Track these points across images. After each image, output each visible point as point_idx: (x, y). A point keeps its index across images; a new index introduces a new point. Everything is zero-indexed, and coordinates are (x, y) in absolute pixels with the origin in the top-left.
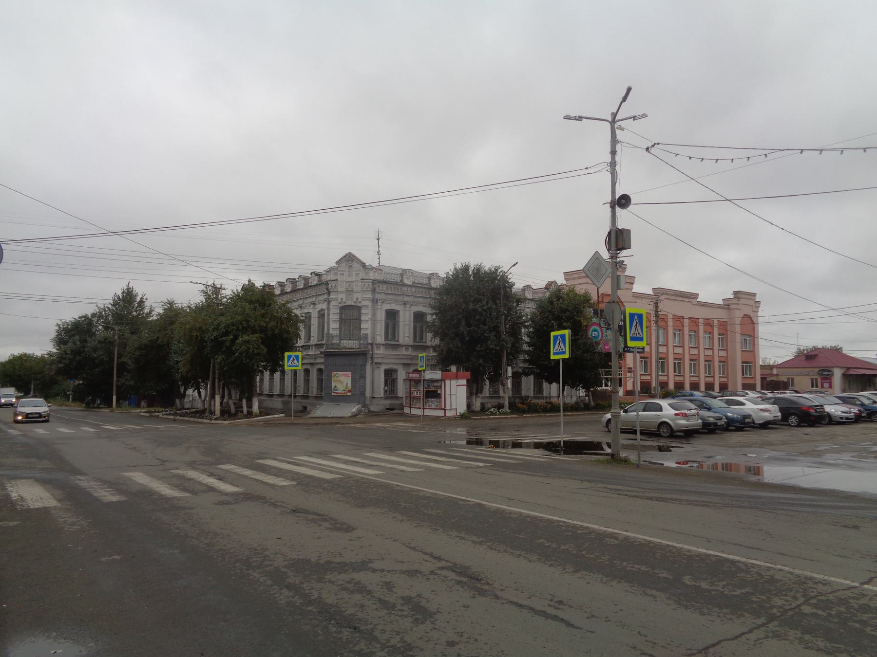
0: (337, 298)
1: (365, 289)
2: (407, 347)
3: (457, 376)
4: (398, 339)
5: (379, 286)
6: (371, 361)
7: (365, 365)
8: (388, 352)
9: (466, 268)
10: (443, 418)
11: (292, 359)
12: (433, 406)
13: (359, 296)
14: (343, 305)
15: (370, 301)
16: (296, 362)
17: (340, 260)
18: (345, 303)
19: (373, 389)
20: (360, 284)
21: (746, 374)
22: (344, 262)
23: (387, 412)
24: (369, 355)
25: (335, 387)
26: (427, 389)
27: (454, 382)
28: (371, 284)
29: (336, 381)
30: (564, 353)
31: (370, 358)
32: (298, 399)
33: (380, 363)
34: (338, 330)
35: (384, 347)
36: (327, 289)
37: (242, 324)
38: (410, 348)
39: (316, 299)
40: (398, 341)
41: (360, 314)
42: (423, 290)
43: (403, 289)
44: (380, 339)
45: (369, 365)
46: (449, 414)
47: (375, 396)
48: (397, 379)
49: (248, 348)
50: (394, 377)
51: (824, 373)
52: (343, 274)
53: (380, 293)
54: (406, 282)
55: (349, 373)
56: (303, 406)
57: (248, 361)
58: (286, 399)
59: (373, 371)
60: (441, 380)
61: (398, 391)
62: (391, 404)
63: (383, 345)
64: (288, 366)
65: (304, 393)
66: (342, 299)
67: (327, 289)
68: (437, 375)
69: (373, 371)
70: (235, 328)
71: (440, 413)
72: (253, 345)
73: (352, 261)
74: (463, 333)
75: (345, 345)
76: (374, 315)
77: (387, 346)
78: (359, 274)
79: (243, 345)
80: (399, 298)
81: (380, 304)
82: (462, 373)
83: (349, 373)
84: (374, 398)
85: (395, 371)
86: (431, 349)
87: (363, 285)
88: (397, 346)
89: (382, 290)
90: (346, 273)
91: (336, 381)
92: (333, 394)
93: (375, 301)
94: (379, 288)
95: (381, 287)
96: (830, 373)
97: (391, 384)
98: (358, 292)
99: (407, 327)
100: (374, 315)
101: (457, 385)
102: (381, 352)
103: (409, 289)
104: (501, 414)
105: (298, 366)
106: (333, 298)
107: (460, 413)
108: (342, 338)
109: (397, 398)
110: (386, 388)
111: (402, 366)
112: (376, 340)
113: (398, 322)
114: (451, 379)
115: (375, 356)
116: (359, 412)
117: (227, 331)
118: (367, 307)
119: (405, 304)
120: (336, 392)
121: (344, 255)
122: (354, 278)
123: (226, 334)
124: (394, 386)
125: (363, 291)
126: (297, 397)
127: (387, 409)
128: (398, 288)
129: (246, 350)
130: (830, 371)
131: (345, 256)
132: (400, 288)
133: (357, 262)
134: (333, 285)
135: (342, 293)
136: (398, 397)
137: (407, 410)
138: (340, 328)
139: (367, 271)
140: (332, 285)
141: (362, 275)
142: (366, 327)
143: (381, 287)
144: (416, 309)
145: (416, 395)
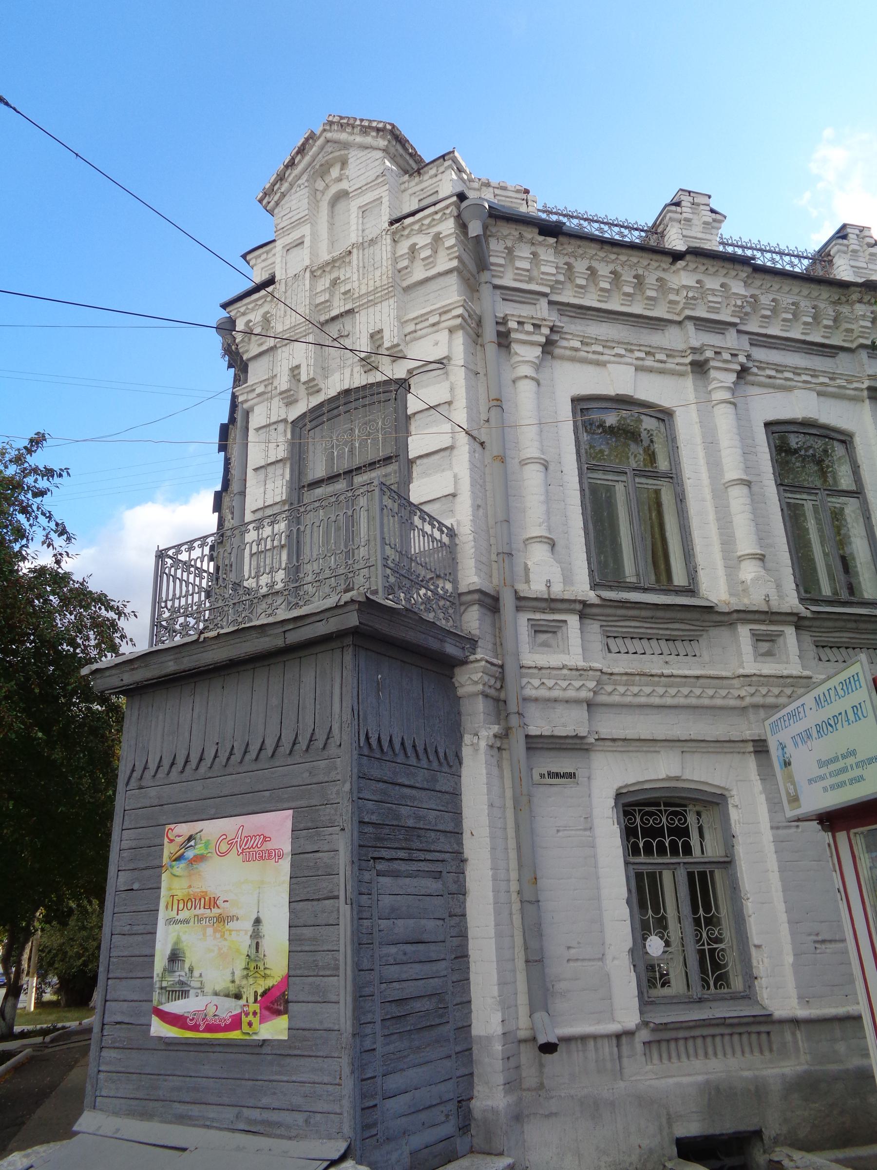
1: (419, 273)
4: (692, 572)
5: (510, 251)
6: (496, 729)
8: (621, 664)
17: (281, 178)
18: (312, 387)
25: (175, 957)
28: (448, 226)
45: (482, 757)
48: (728, 863)
53: (508, 293)
61: (761, 963)
63: (584, 610)
73: (344, 163)
92: (159, 1028)
97: (686, 908)
99: (738, 499)
102: (575, 658)
103: (713, 283)
110: (655, 945)
112: (527, 569)
113: (673, 477)
124: (712, 922)
125: (407, 289)
131: (302, 150)
136: (768, 1019)
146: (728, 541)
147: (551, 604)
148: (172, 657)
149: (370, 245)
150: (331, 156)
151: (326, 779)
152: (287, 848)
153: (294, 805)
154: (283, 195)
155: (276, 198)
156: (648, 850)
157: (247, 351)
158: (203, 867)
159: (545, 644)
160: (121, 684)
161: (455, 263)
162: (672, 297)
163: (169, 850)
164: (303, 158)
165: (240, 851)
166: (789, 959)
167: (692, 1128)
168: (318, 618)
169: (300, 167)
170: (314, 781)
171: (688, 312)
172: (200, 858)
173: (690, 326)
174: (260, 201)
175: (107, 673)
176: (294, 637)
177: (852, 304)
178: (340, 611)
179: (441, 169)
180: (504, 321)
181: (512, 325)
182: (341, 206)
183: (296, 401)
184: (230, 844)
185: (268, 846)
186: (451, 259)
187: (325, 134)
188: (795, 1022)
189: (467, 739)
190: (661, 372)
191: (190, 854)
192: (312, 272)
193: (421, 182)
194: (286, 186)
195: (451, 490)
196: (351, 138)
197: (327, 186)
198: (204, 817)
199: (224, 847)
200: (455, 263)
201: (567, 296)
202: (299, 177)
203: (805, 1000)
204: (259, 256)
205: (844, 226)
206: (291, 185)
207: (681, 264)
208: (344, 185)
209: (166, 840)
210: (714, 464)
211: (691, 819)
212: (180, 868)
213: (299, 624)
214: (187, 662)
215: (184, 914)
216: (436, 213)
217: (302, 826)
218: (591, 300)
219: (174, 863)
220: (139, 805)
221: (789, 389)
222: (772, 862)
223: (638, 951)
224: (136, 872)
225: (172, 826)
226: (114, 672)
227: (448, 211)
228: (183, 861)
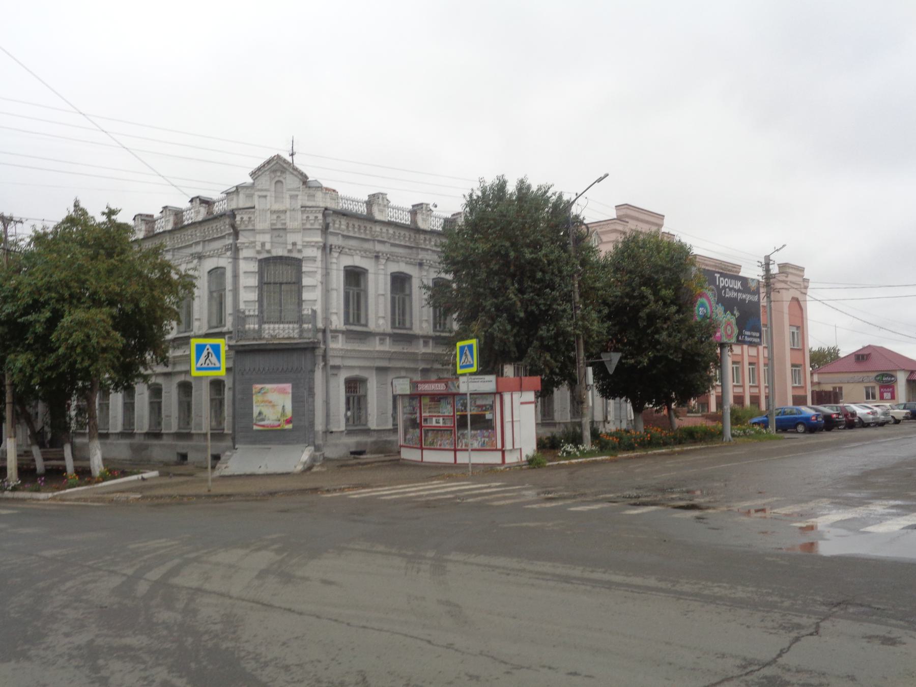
0: (254, 242)
1: (308, 226)
2: (383, 336)
3: (521, 387)
6: (323, 363)
7: (313, 371)
9: (501, 186)
10: (502, 468)
11: (205, 353)
12: (476, 445)
13: (298, 238)
14: (265, 255)
15: (318, 248)
16: (213, 359)
17: (259, 169)
18: (269, 252)
19: (328, 416)
20: (298, 215)
21: (795, 383)
22: (268, 173)
23: (355, 458)
24: (319, 352)
25: (260, 413)
26: (462, 411)
27: (516, 395)
28: (320, 216)
29: (263, 402)
30: (472, 366)
31: (321, 358)
32: (165, 441)
33: (338, 368)
34: (257, 304)
35: (344, 336)
36: (233, 226)
37: (69, 288)
38: (388, 340)
39: (204, 247)
40: (366, 325)
41: (299, 273)
42: (407, 234)
43: (374, 229)
44: (337, 322)
45: (320, 370)
46: (511, 459)
47: (334, 430)
48: (365, 396)
49: (88, 336)
50: (361, 392)
51: (884, 379)
52: (265, 197)
54: (378, 216)
55: (288, 387)
56: (178, 454)
57: (86, 363)
58: (137, 440)
59: (327, 382)
60: (494, 394)
61: (370, 418)
62: (358, 444)
63: (343, 332)
64: (198, 369)
65: (179, 428)
66: (263, 244)
67: (233, 226)
68: (488, 383)
69: (327, 382)
70: (53, 295)
71: (494, 458)
72: (97, 330)
74: (514, 304)
75: (277, 331)
76: (327, 274)
77: (350, 335)
78: (297, 196)
79: (76, 331)
80: (367, 246)
81: (335, 255)
82: (527, 380)
83: (288, 387)
84: (332, 432)
85: (362, 381)
86: (421, 341)
87: (305, 217)
88: (365, 336)
89: (339, 229)
90: (271, 194)
91: (263, 402)
92: (255, 428)
93: (326, 249)
94: (334, 224)
95: (337, 222)
96: (893, 379)
98: (294, 231)
99: (381, 299)
100: (327, 274)
101: (522, 403)
103: (384, 230)
104: (584, 454)
105: (219, 368)
106: (244, 243)
107: (527, 456)
108: (265, 319)
109: (368, 431)
110: (349, 413)
111: (374, 372)
112: (331, 322)
113: (366, 291)
114: (512, 391)
115: (330, 353)
116: (313, 459)
117: (36, 302)
118: (314, 259)
119: (377, 257)
120: (262, 423)
121: (267, 157)
122: (286, 204)
123: (36, 306)
125: (304, 229)
126: (165, 437)
127: (352, 453)
128: (365, 227)
129: (83, 341)
130: (892, 376)
131: (269, 162)
132: (369, 226)
133: (292, 174)
134: (246, 218)
135: (263, 232)
137: (409, 454)
138: (260, 301)
139: (312, 191)
140: (242, 218)
141: (302, 200)
142: (312, 296)
143: (337, 222)
144: (394, 268)
145: (434, 424)
146: (377, 312)
147: (336, 331)
152: (290, 391)
154: (259, 176)
156: (348, 392)
159: (333, 341)
161: (321, 227)
162: (373, 233)
163: (254, 391)
166: (376, 417)
167: (353, 450)
169: (266, 169)
171: (376, 238)
172: (265, 393)
173: (376, 242)
174: (251, 176)
177: (420, 234)
180: (331, 245)
181: (333, 247)
182: (279, 185)
188: (374, 430)
189: (317, 366)
190: (366, 257)
192: (271, 212)
194: (260, 173)
195: (315, 299)
196: (288, 168)
197: (275, 177)
200: (321, 227)
201: (345, 233)
202: (265, 171)
203: (377, 425)
205: (422, 204)
206: (263, 173)
207: (377, 224)
208: (281, 179)
210: (377, 289)
211: (358, 384)
212: (259, 394)
215: (262, 404)
218: (351, 234)
221: (398, 262)
222: (375, 396)
223: (346, 415)
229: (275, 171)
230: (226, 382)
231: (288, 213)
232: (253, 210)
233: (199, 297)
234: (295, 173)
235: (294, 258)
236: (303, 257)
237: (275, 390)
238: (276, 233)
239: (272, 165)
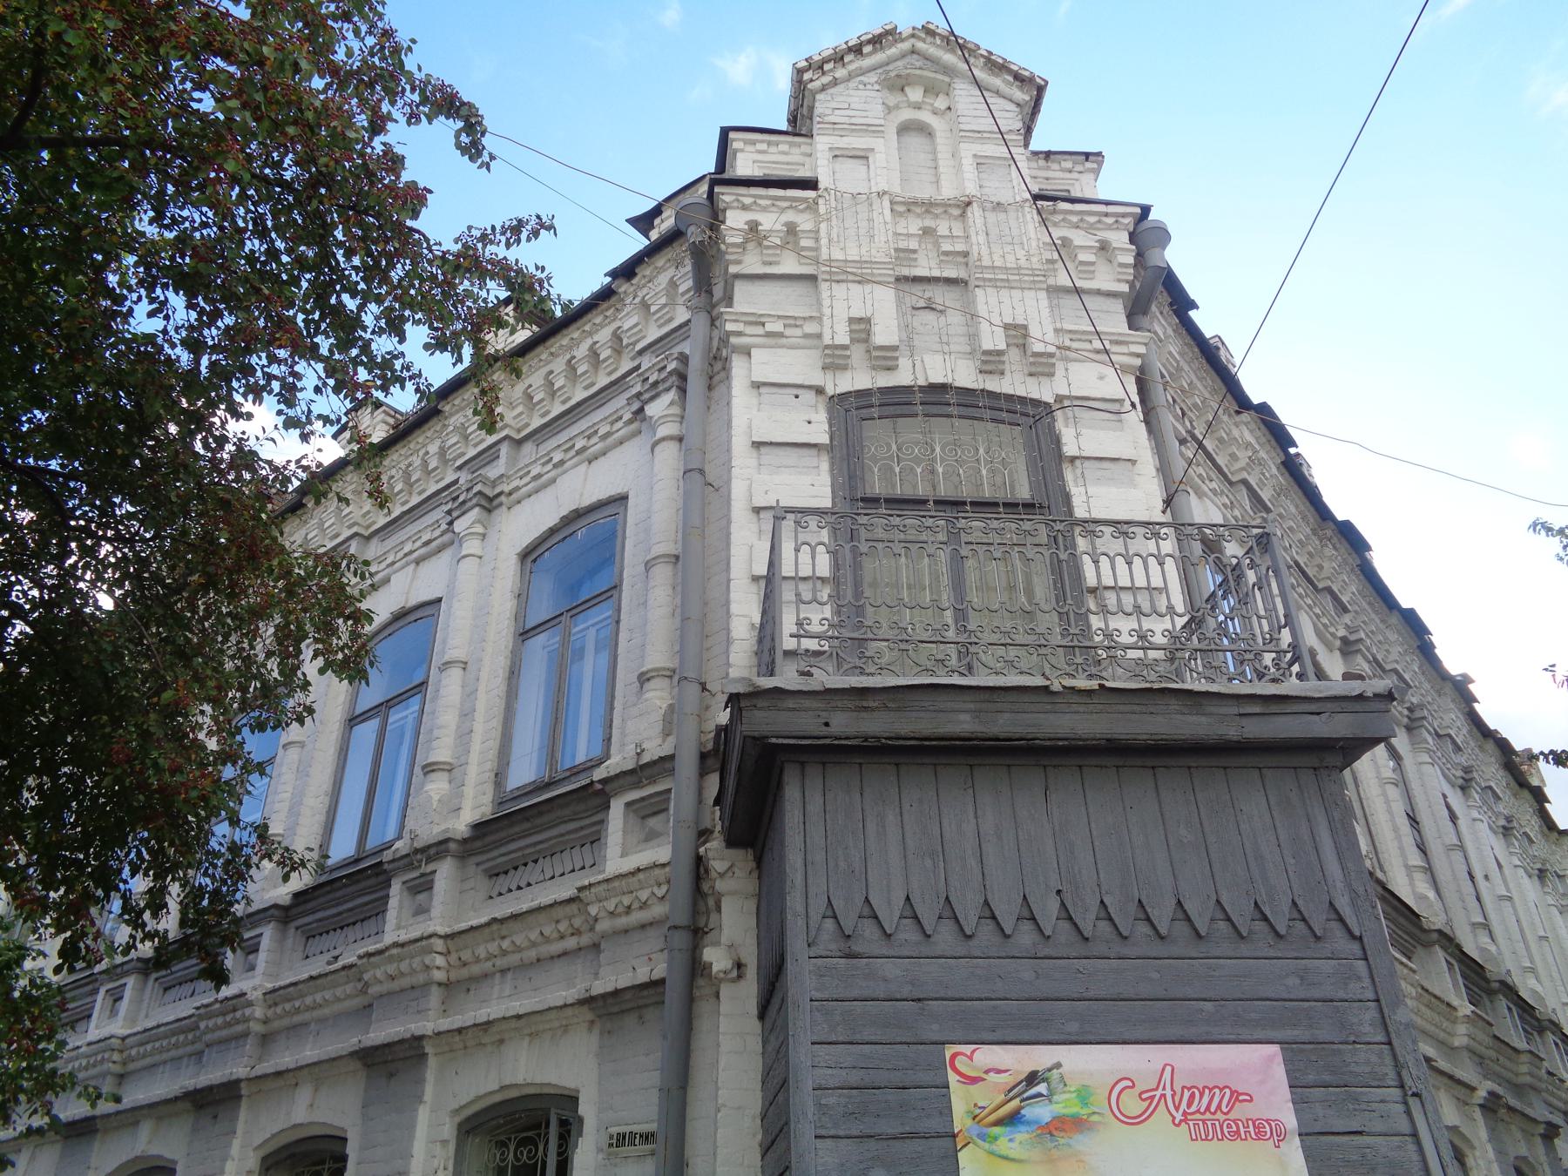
17: (838, 58)
18: (885, 358)
22: (872, 78)
28: (1120, 239)
52: (862, 157)
118: (1111, 408)
131: (877, 41)
134: (769, 222)
148: (972, 706)
149: (994, 209)
150: (918, 72)
151: (1341, 994)
152: (1290, 1121)
153: (1278, 1035)
154: (835, 82)
155: (826, 79)
157: (739, 262)
158: (1081, 1142)
160: (824, 731)
163: (961, 1100)
164: (874, 51)
165: (1179, 1116)
168: (1313, 707)
170: (1317, 994)
175: (790, 703)
176: (1257, 729)
178: (1358, 706)
179: (1079, 168)
182: (915, 141)
183: (844, 368)
184: (1147, 1097)
185: (1241, 1111)
186: (1119, 281)
187: (912, 41)
191: (1041, 1112)
193: (1048, 168)
194: (840, 73)
198: (1051, 1038)
199: (1133, 1106)
204: (753, 143)
206: (850, 77)
208: (925, 116)
209: (952, 1078)
212: (1013, 1142)
213: (1274, 708)
214: (1005, 724)
216: (1107, 215)
217: (1311, 1078)
219: (997, 1130)
220: (855, 993)
224: (872, 1144)
225: (967, 1049)
226: (807, 703)
227: (1126, 221)
228: (1022, 1128)
229: (898, 85)
230: (586, 1109)
231: (975, 212)
232: (810, 194)
233: (465, 665)
234: (996, 82)
235: (1010, 398)
236: (1059, 399)
237: (1150, 1099)
238: (919, 294)
239: (893, 51)
